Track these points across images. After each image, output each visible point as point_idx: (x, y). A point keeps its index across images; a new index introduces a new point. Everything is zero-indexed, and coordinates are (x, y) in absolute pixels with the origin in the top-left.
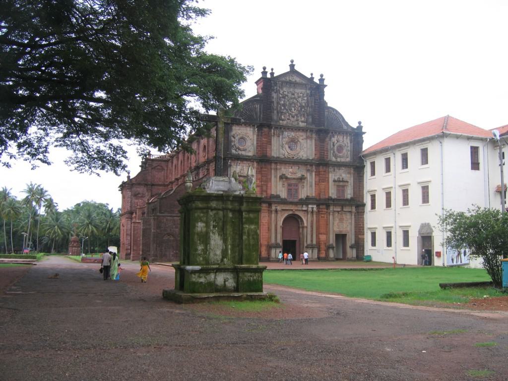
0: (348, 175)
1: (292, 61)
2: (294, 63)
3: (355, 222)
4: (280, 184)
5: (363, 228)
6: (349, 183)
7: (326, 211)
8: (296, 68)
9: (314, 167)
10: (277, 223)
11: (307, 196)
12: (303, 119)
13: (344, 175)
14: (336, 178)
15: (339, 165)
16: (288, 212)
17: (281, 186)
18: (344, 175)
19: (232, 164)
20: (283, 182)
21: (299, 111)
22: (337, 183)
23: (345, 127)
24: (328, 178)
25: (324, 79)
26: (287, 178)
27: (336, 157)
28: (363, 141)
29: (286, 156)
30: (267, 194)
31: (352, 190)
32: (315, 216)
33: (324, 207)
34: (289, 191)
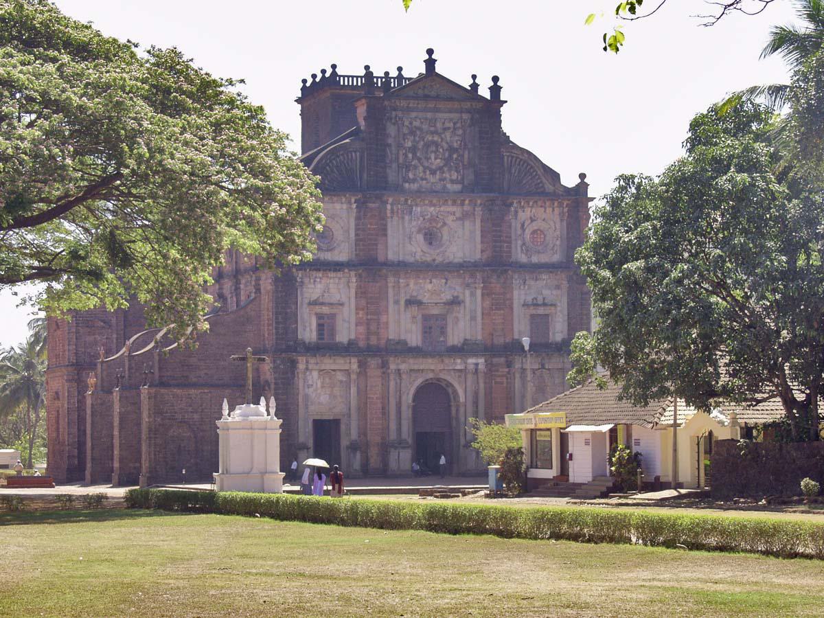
0: (555, 292)
1: (430, 52)
2: (433, 57)
6: (559, 308)
8: (439, 69)
10: (400, 397)
11: (466, 340)
12: (455, 176)
13: (546, 292)
18: (546, 292)
19: (306, 280)
21: (447, 161)
24: (511, 299)
26: (419, 303)
27: (527, 251)
31: (566, 324)
34: (427, 331)
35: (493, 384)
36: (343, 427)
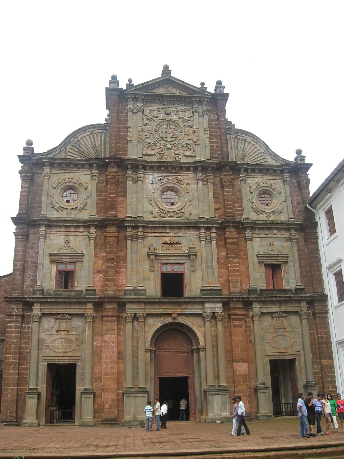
0: (286, 244)
3: (310, 334)
4: (147, 265)
5: (328, 343)
6: (290, 258)
7: (242, 312)
8: (172, 75)
9: (214, 231)
13: (277, 244)
14: (261, 253)
15: (267, 226)
16: (162, 319)
17: (147, 267)
20: (152, 261)
22: (262, 260)
23: (271, 162)
25: (224, 87)
28: (309, 181)
29: (155, 214)
30: (116, 285)
32: (220, 324)
33: (240, 305)
35: (232, 327)
36: (79, 371)
